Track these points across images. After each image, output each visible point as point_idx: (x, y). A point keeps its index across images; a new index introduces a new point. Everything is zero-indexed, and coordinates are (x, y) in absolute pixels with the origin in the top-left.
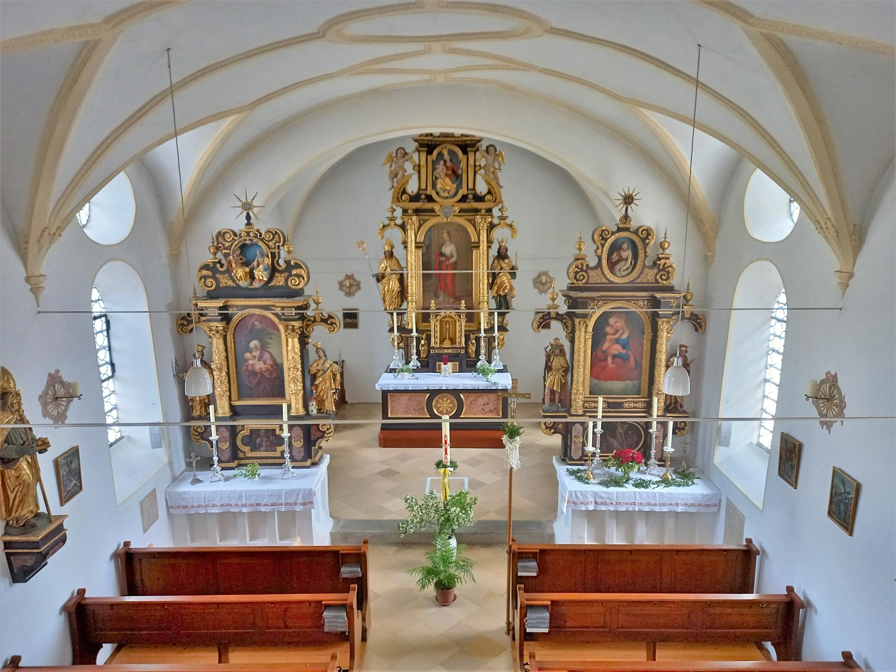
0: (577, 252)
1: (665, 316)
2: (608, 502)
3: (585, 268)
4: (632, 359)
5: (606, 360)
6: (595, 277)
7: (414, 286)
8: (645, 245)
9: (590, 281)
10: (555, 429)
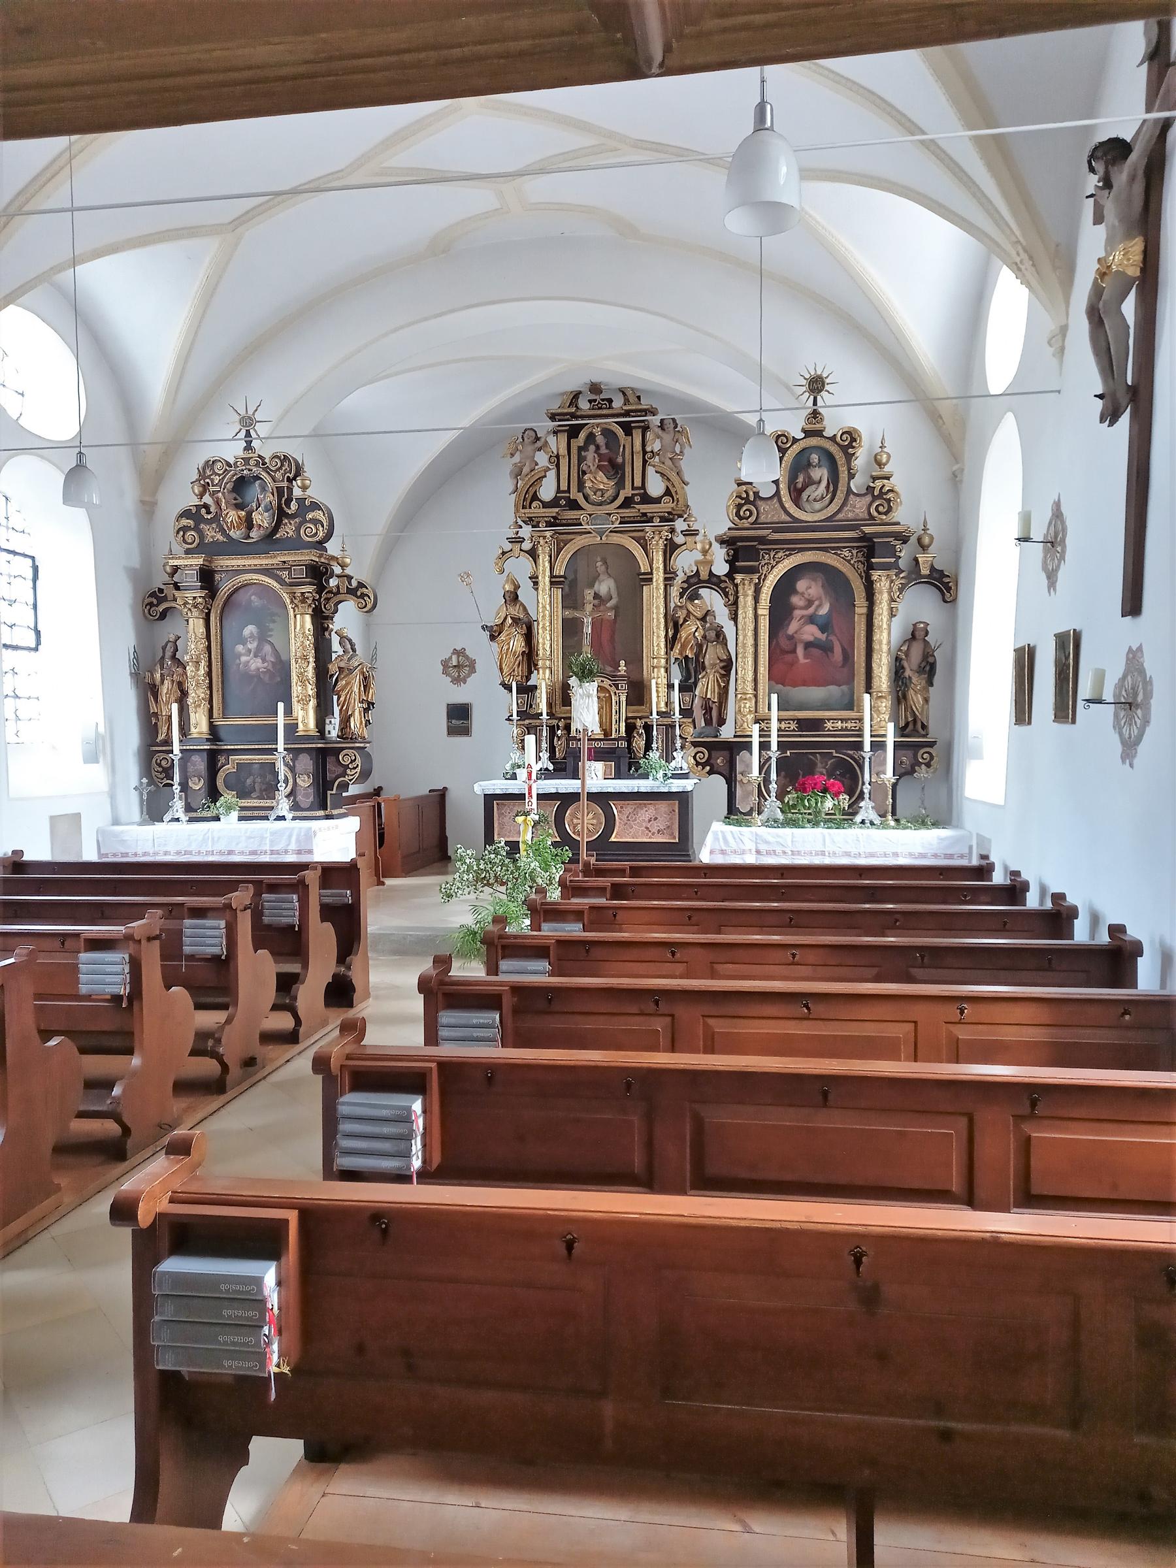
2: (779, 849)
3: (752, 499)
4: (838, 650)
5: (794, 651)
6: (770, 513)
7: (548, 641)
8: (849, 457)
9: (762, 519)
10: (712, 766)
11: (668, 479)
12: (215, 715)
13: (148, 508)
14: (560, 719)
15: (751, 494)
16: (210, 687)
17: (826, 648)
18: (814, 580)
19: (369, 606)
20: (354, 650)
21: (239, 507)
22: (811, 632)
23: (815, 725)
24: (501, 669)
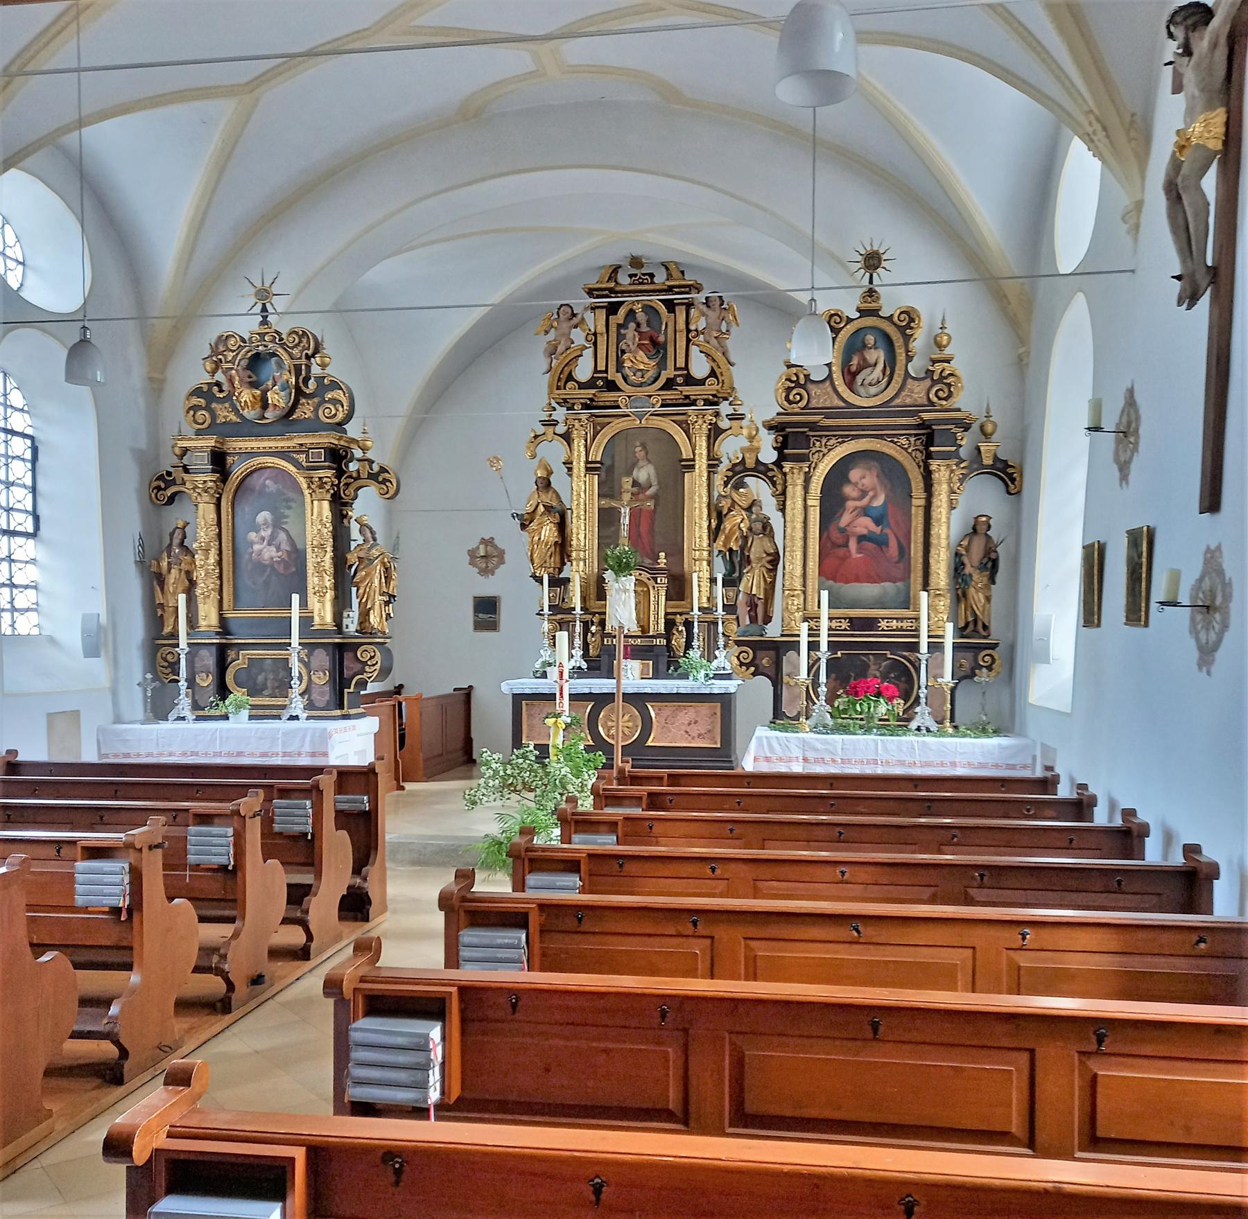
2: (828, 757)
4: (893, 543)
5: (846, 545)
6: (821, 397)
8: (907, 338)
9: (814, 403)
10: (757, 667)
11: (714, 360)
12: (225, 607)
13: (156, 386)
14: (594, 614)
15: (802, 377)
16: (220, 577)
17: (881, 542)
18: (869, 469)
19: (391, 492)
20: (375, 539)
21: (254, 385)
23: (869, 624)
24: (532, 561)
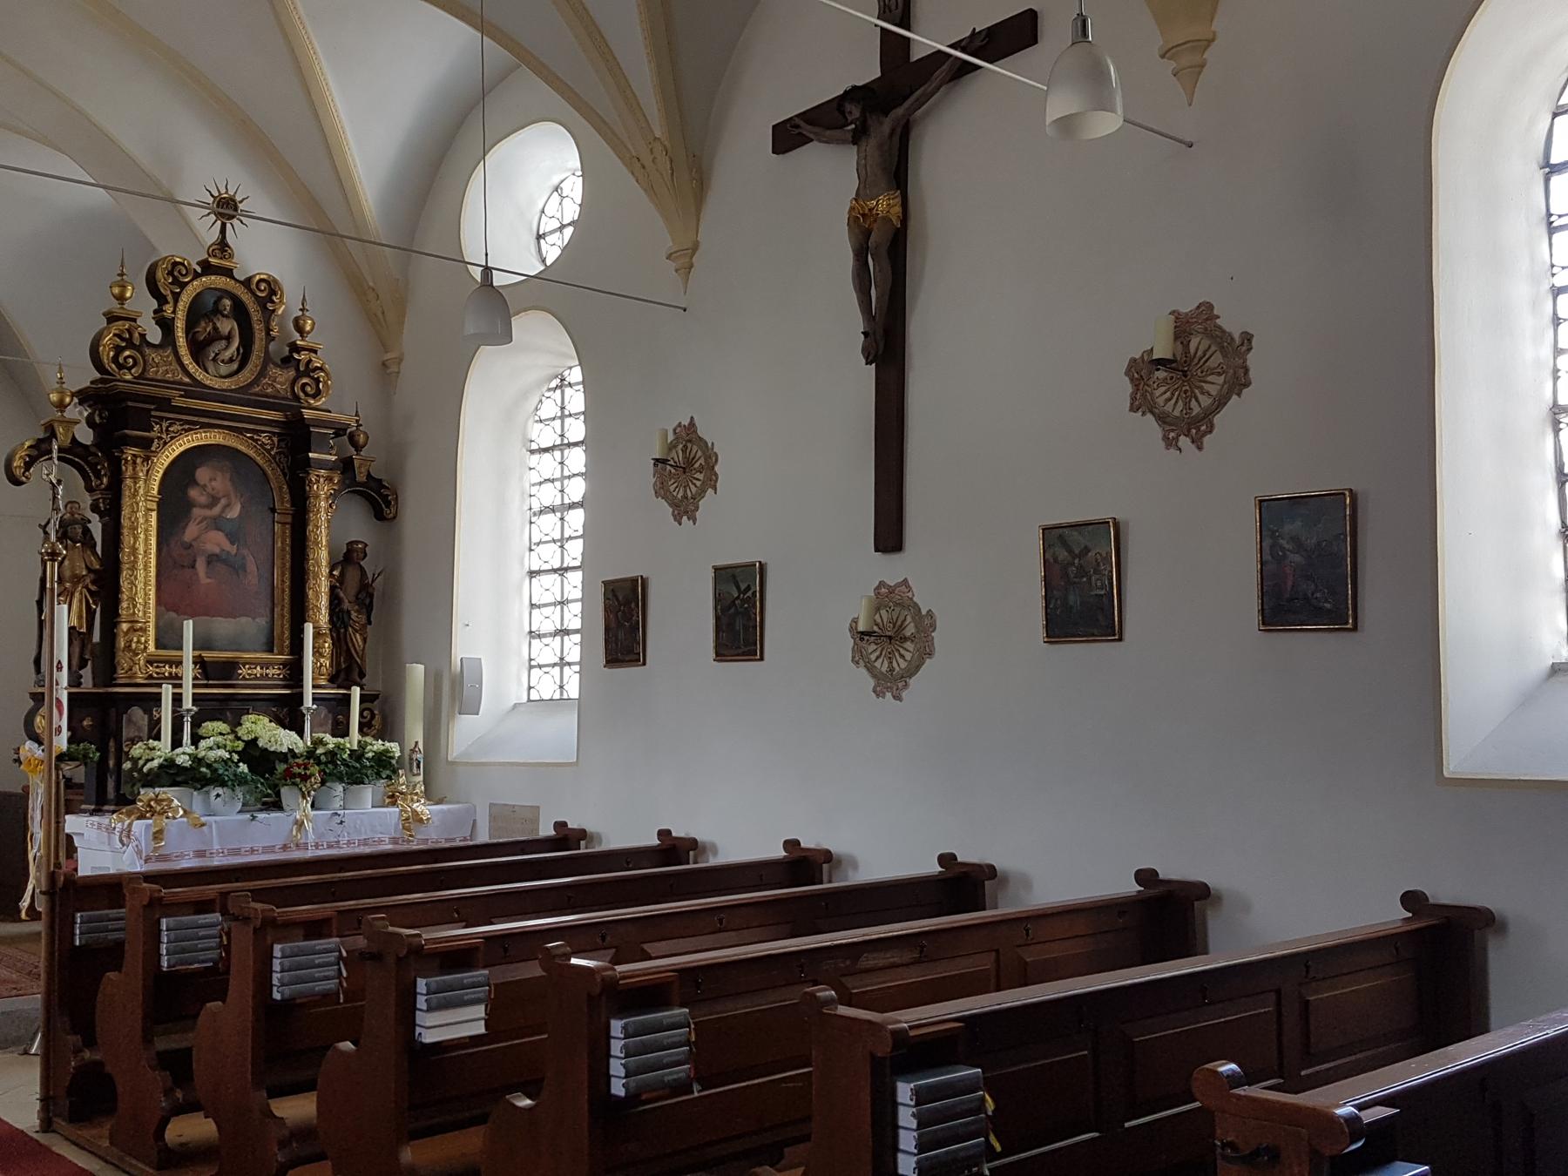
0: (115, 304)
1: (322, 464)
6: (160, 366)
8: (268, 315)
22: (216, 542)
